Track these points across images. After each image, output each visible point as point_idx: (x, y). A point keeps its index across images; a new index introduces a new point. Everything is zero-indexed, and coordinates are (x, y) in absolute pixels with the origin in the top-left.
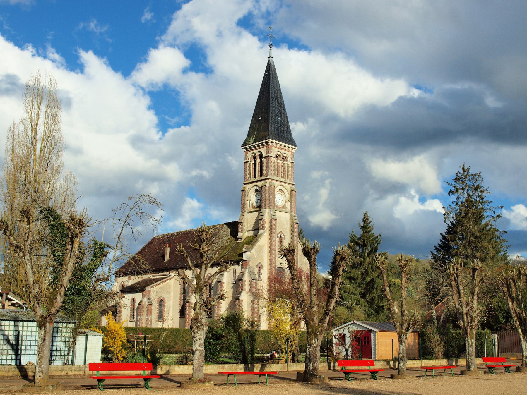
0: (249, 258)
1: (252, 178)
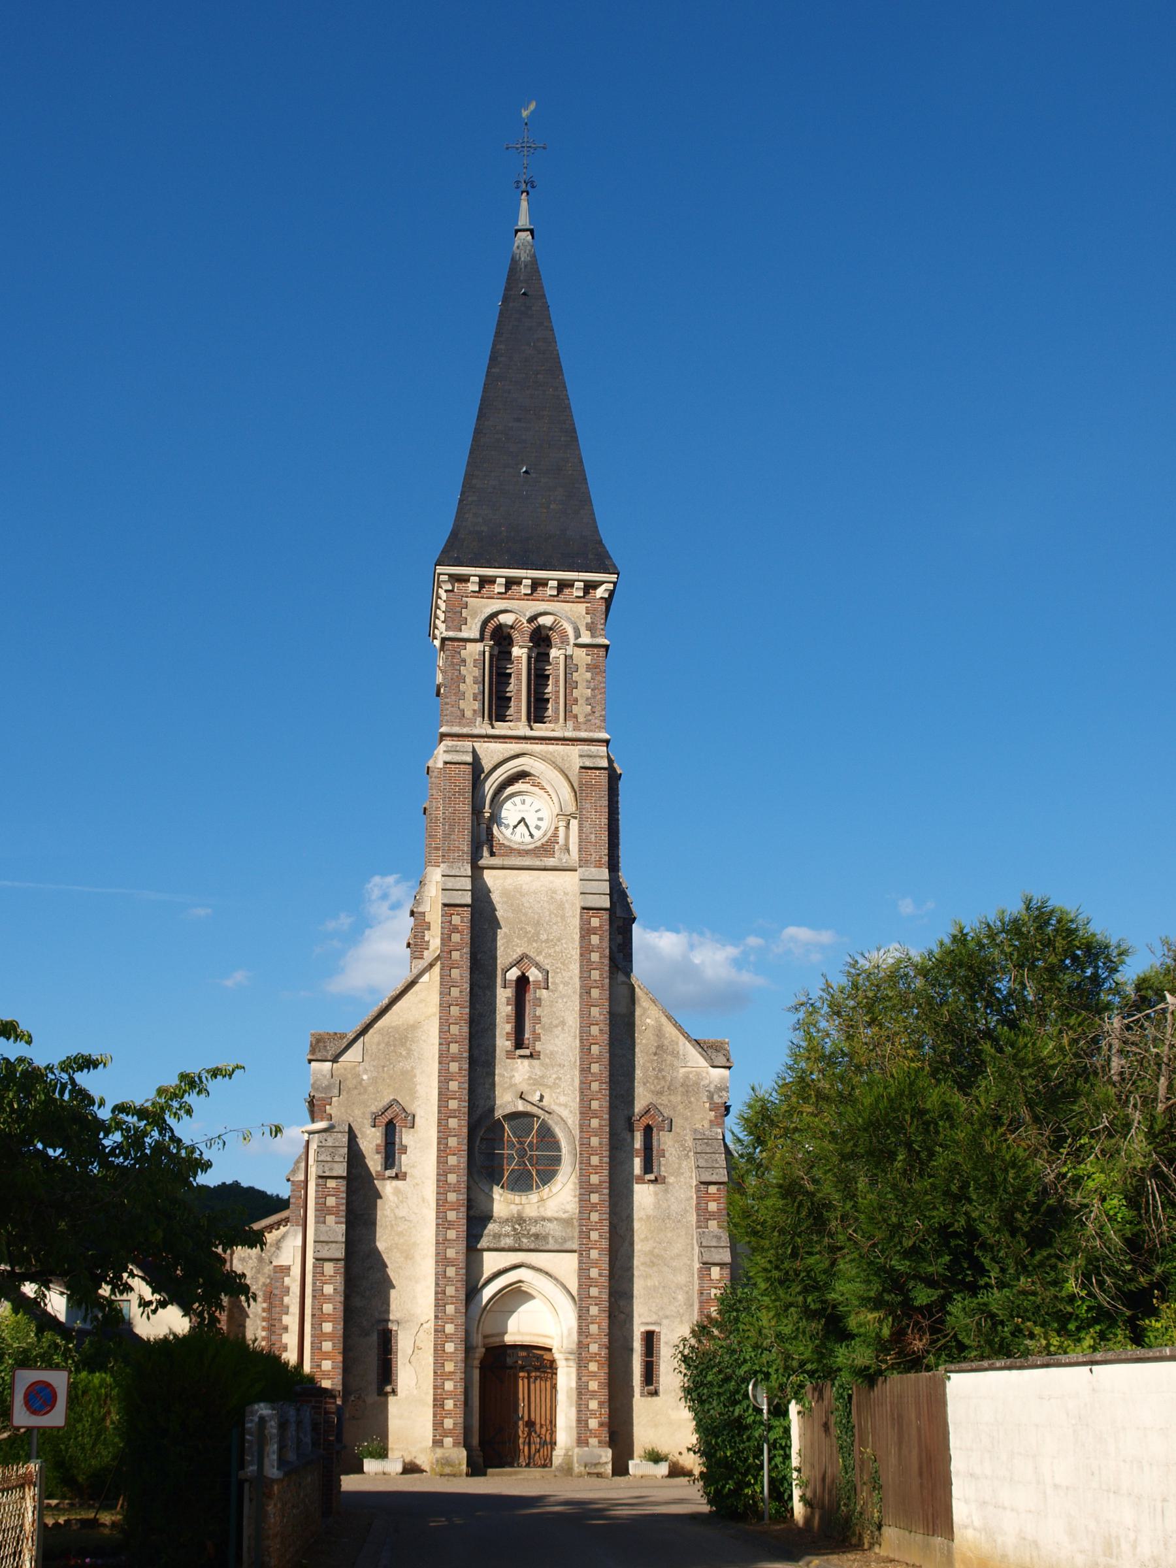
0: (328, 1088)
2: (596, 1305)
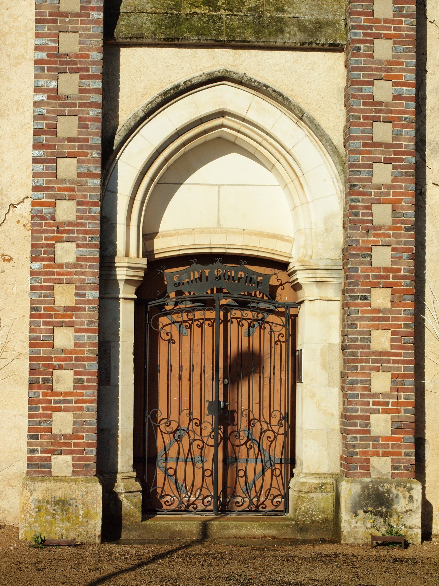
2: (387, 161)
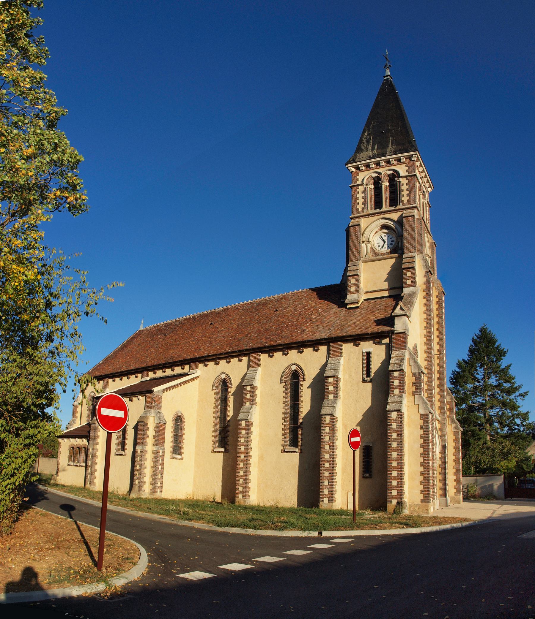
1: (371, 209)
